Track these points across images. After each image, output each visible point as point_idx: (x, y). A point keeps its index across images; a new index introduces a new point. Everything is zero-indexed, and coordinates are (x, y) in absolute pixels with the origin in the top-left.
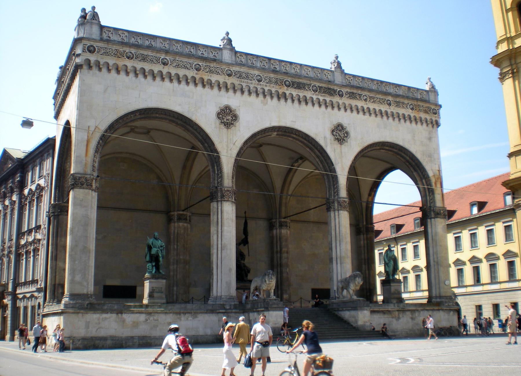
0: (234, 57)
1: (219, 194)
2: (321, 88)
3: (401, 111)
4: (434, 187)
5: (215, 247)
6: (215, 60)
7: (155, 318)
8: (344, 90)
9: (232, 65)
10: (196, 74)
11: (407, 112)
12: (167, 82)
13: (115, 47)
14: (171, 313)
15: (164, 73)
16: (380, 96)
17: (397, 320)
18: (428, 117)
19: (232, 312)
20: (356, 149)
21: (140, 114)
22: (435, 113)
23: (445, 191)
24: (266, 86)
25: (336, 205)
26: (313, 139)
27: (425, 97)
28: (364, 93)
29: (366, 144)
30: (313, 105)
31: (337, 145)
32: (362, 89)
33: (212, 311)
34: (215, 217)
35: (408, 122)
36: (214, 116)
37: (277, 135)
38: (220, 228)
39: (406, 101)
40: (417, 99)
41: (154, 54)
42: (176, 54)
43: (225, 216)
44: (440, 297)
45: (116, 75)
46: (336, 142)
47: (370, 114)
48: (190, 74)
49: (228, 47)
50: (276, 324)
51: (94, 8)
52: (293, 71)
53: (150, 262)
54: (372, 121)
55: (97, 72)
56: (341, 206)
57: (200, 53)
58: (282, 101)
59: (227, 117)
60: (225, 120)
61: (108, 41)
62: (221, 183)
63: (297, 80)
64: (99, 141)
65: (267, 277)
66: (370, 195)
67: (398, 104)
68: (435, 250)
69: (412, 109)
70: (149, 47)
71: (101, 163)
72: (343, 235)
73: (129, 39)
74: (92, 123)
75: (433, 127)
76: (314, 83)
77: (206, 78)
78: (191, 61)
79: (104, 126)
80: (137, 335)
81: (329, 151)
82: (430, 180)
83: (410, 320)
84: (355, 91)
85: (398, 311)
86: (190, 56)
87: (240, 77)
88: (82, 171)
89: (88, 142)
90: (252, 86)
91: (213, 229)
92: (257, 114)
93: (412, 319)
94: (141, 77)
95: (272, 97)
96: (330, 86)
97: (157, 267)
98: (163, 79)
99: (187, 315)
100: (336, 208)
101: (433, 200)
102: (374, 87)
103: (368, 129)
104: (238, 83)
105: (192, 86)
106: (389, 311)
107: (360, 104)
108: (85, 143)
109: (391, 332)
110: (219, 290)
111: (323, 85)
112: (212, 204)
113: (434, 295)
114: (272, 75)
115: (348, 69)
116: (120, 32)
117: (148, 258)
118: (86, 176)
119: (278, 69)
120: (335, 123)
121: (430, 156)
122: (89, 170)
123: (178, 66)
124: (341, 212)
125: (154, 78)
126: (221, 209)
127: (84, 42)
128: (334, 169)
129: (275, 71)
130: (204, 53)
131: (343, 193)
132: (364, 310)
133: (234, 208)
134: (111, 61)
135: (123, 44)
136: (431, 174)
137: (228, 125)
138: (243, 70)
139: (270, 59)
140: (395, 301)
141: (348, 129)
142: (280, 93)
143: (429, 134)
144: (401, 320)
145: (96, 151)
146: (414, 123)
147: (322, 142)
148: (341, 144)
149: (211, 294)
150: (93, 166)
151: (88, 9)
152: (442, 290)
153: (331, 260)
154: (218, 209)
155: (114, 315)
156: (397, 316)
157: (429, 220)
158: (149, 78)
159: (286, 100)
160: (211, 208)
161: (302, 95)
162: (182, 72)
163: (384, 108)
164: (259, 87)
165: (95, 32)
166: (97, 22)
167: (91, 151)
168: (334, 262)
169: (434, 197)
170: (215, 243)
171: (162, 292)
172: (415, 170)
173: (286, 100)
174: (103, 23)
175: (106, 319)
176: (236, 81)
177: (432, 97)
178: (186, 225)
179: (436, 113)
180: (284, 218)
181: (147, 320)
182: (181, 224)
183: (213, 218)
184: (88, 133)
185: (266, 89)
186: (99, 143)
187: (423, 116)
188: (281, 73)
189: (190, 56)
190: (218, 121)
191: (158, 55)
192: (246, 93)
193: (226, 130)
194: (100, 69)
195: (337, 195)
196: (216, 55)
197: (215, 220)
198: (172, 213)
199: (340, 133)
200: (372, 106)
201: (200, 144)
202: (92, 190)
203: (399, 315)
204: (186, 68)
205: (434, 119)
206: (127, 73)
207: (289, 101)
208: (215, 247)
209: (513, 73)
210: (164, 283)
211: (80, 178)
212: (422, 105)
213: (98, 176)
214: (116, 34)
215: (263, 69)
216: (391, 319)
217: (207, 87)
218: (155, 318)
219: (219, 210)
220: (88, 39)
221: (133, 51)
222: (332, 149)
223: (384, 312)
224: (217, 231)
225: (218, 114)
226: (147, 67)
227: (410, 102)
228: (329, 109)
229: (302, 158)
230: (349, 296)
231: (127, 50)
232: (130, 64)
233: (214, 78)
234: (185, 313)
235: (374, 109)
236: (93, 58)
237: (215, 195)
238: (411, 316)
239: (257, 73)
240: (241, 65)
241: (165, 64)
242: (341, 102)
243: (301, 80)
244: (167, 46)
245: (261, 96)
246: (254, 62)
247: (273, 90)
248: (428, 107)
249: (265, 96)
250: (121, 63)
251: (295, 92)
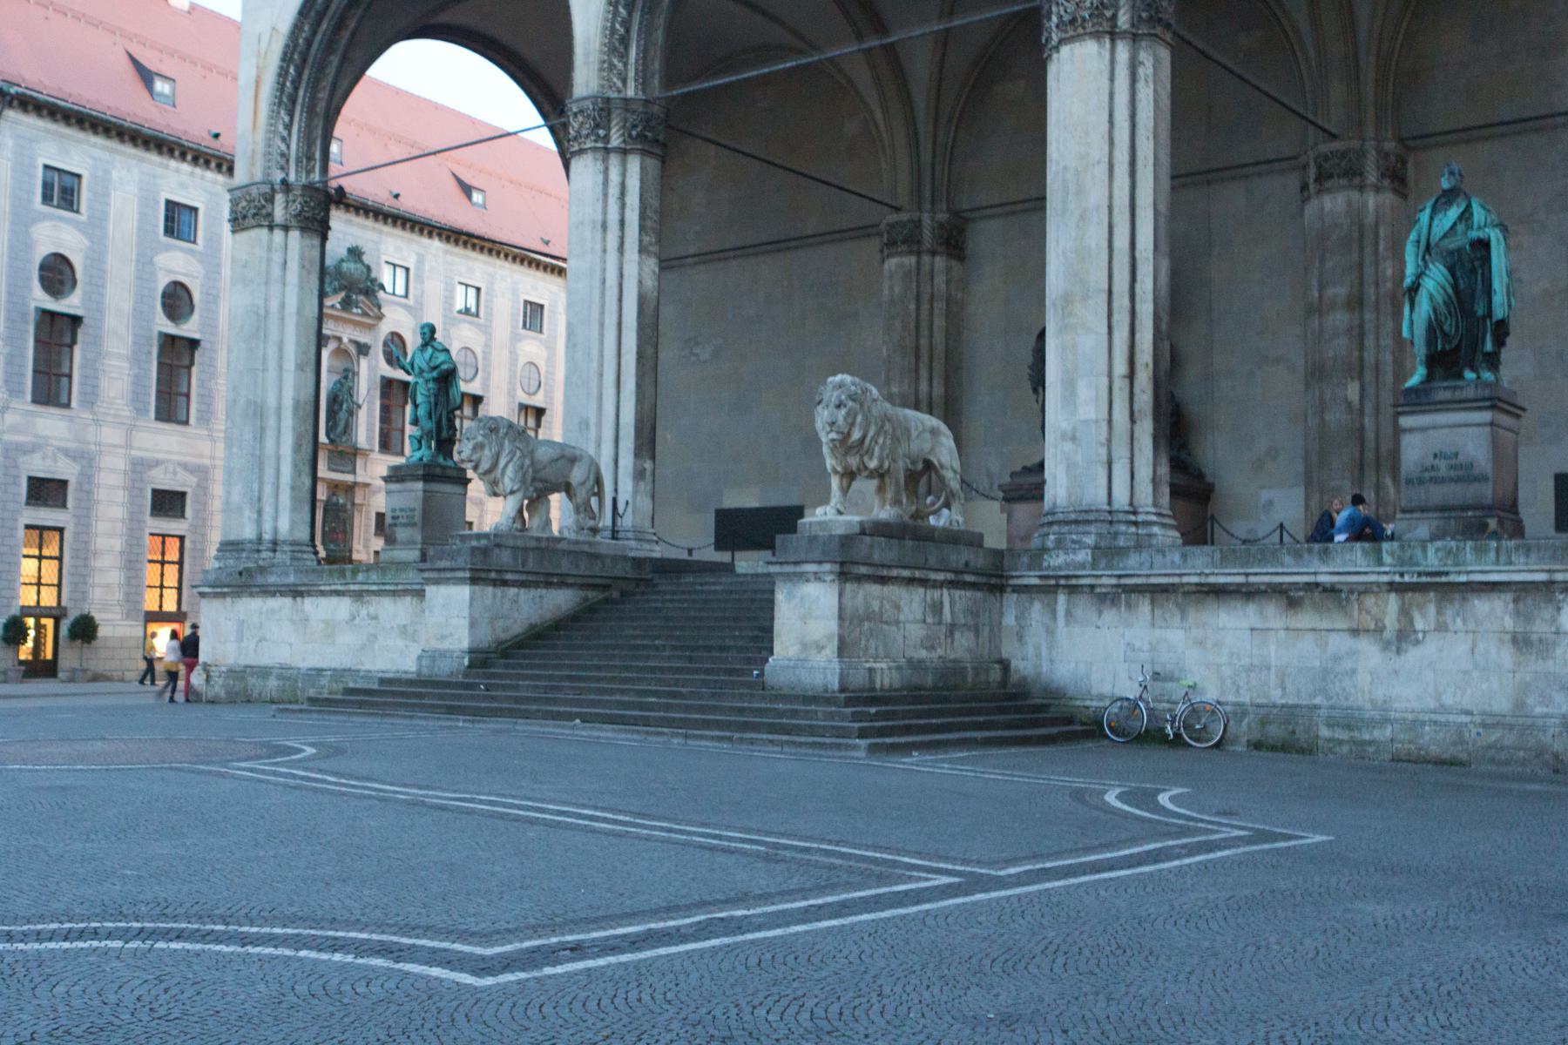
7: (372, 610)
17: (1386, 646)
50: (443, 637)
72: (1070, 176)
80: (333, 666)
83: (1507, 656)
85: (1393, 587)
93: (1521, 642)
106: (1331, 590)
109: (1331, 723)
132: (803, 577)
140: (1423, 530)
144: (1413, 655)
155: (288, 601)
156: (1391, 620)
171: (415, 525)
175: (273, 611)
178: (911, 261)
186: (283, 73)
202: (271, 228)
203: (1405, 612)
210: (420, 494)
216: (1339, 643)
218: (372, 610)
223: (1288, 597)
238: (1509, 623)
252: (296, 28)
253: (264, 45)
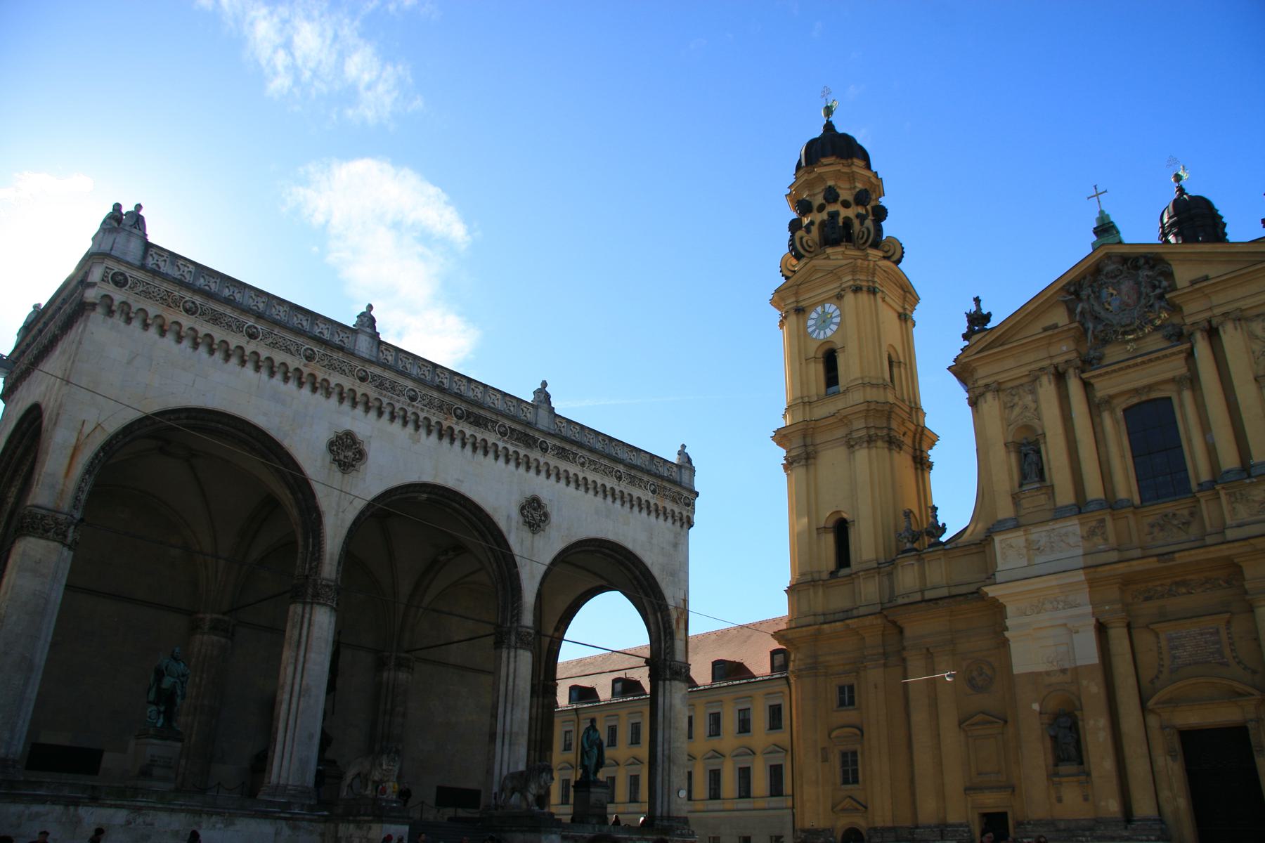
0: (375, 350)
1: (310, 591)
2: (513, 430)
3: (637, 492)
4: (674, 626)
5: (288, 689)
6: (341, 349)
8: (551, 442)
9: (370, 362)
10: (305, 365)
11: (646, 495)
12: (249, 369)
13: (165, 286)
14: (183, 811)
15: (247, 352)
16: (605, 462)
19: (303, 820)
20: (558, 546)
21: (187, 418)
22: (688, 505)
23: (691, 633)
24: (422, 410)
25: (513, 638)
26: (488, 516)
27: (675, 475)
28: (581, 452)
29: (574, 540)
30: (497, 457)
31: (526, 534)
32: (581, 445)
33: (265, 815)
34: (296, 632)
35: (644, 513)
36: (322, 444)
37: (428, 499)
38: (302, 653)
39: (646, 478)
40: (662, 478)
41: (235, 315)
42: (276, 323)
43: (316, 631)
44: (669, 818)
45: (157, 336)
46: (526, 528)
47: (587, 490)
48: (294, 362)
49: (369, 330)
51: (139, 207)
52: (471, 394)
53: (156, 703)
54: (590, 501)
55: (122, 324)
56: (523, 642)
57: (317, 331)
58: (446, 441)
59: (346, 452)
60: (342, 457)
61: (155, 273)
62: (316, 569)
63: (475, 410)
64: (99, 452)
65: (385, 756)
66: (557, 629)
67: (633, 480)
68: (667, 736)
69: (654, 492)
70: (228, 302)
71: (91, 494)
73: (196, 278)
75: (682, 526)
76: (502, 421)
77: (320, 376)
78: (299, 340)
79: (113, 426)
81: (513, 540)
82: (669, 615)
84: (567, 447)
86: (299, 332)
87: (380, 386)
88: (51, 506)
89: (76, 449)
90: (398, 406)
91: (287, 655)
92: (401, 457)
94: (202, 350)
95: (429, 432)
96: (528, 431)
97: (169, 715)
98: (243, 363)
99: (214, 819)
100: (513, 643)
101: (671, 649)
102: (599, 446)
103: (580, 514)
104: (376, 395)
105: (292, 385)
107: (573, 469)
108: (69, 452)
110: (284, 774)
111: (518, 427)
112: (292, 607)
113: (658, 813)
114: (435, 394)
115: (561, 406)
116: (180, 262)
117: (152, 696)
118: (59, 516)
119: (446, 385)
120: (528, 494)
121: (673, 574)
122: (66, 506)
123: (274, 345)
124: (521, 652)
125: (227, 357)
126: (310, 619)
127: (110, 263)
128: (518, 574)
129: (440, 389)
130: (325, 332)
131: (528, 619)
133: (333, 619)
134: (153, 309)
135: (181, 283)
136: (671, 602)
138: (387, 374)
139: (435, 366)
140: (594, 821)
141: (548, 509)
142: (445, 427)
143: (677, 535)
145: (89, 471)
146: (653, 514)
147: (502, 525)
148: (534, 533)
149: (266, 780)
150: (76, 498)
151: (127, 208)
152: (673, 807)
153: (493, 736)
154: (303, 617)
157: (661, 683)
158: (218, 356)
159: (452, 440)
160: (291, 613)
161: (479, 436)
162: (279, 357)
163: (610, 483)
164: (410, 410)
165: (133, 251)
166: (141, 233)
167: (78, 470)
168: (499, 741)
169: (673, 644)
170: (289, 681)
172: (647, 595)
173: (452, 440)
174: (151, 239)
176: (373, 393)
177: (685, 478)
178: (223, 640)
179: (690, 505)
180: (407, 652)
181: (129, 823)
182: (215, 638)
183: (291, 633)
184: (80, 432)
185: (422, 415)
186: (97, 455)
187: (670, 506)
188: (450, 394)
189: (299, 332)
190: (329, 457)
191: (243, 318)
192: (386, 416)
193: (340, 474)
194: (128, 320)
195: (518, 620)
196: (346, 340)
197: (296, 636)
198: (201, 616)
199: (534, 513)
200: (591, 477)
201: (288, 492)
202: (65, 545)
204: (288, 350)
205: (685, 514)
206: (179, 339)
207: (458, 443)
208: (288, 689)
209: (807, 459)
211: (43, 517)
212: (667, 487)
213: (82, 520)
214: (173, 263)
215: (420, 381)
217: (319, 391)
218: (149, 819)
219: (306, 621)
220: (118, 260)
221: (198, 300)
222: (518, 539)
224: (296, 660)
225: (331, 444)
226: (218, 334)
227: (652, 480)
228: (522, 469)
229: (459, 548)
230: (524, 806)
231: (188, 296)
232: (187, 322)
233: (335, 379)
234: (210, 814)
235: (594, 482)
236: (118, 296)
237: (303, 590)
239: (410, 384)
240: (385, 366)
241: (252, 336)
242: (542, 461)
243: (482, 412)
244: (261, 306)
245: (411, 427)
246: (408, 366)
247: (434, 420)
248: (679, 493)
249: (417, 427)
250: (171, 316)
251: (469, 431)
252: (116, 436)
253: (88, 429)
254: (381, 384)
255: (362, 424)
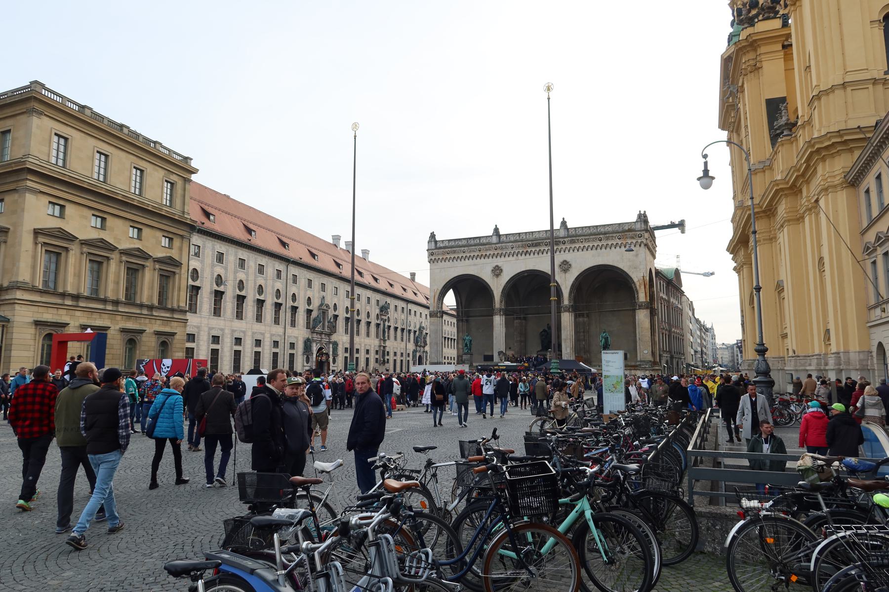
18: (634, 241)
31: (563, 274)
56: (567, 310)
61: (441, 248)
67: (608, 239)
74: (435, 288)
92: (513, 266)
120: (562, 260)
129: (522, 241)
131: (566, 302)
136: (635, 280)
137: (497, 276)
189: (475, 245)
199: (566, 266)
254: (502, 249)
255: (499, 261)
